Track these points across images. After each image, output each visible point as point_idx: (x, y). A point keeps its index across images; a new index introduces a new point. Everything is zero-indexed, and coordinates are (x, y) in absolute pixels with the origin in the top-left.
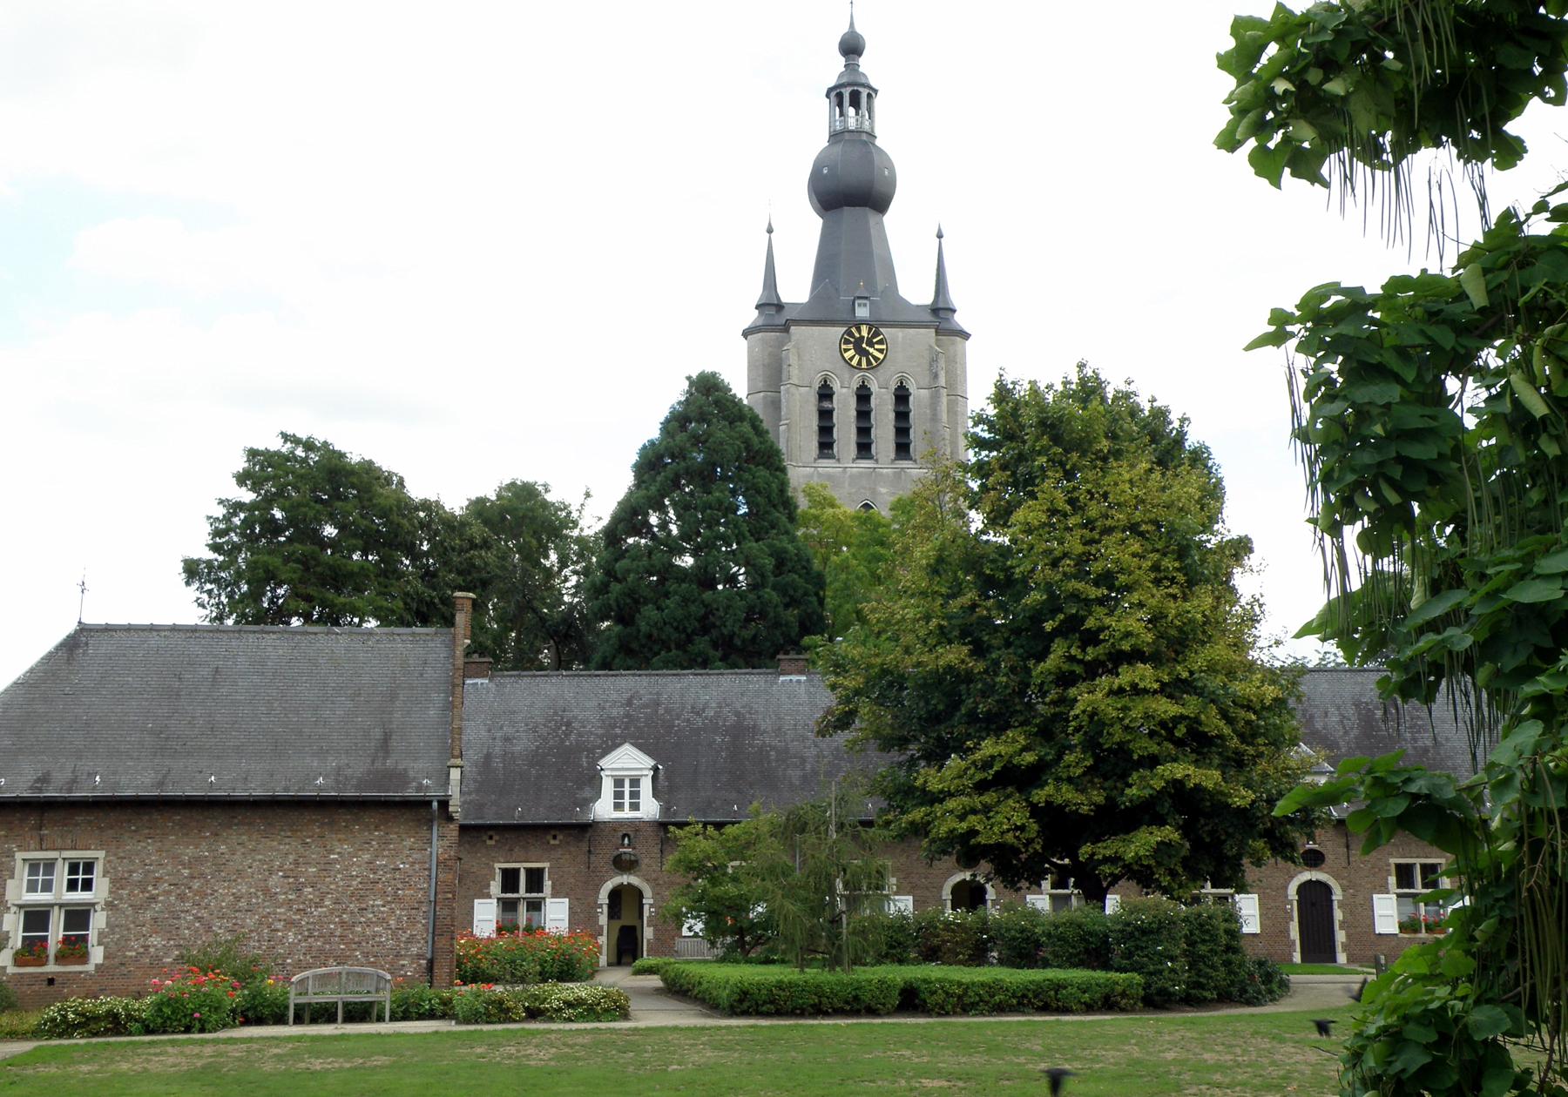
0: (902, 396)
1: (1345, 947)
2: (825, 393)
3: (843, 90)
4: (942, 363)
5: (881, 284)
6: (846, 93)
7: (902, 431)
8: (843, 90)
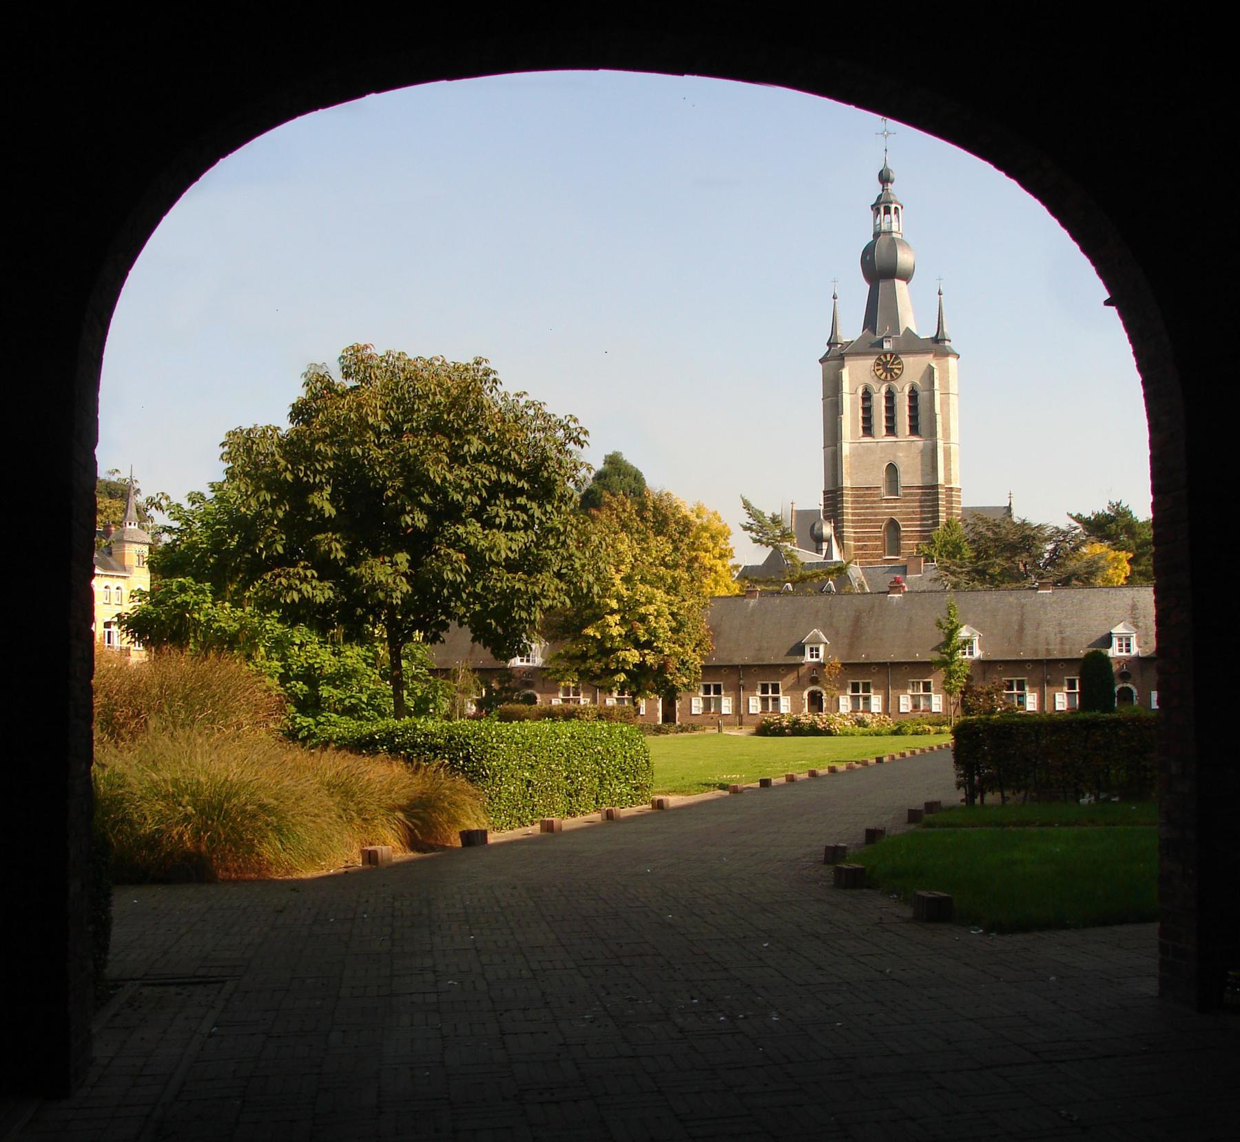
0: (913, 396)
2: (867, 396)
7: (914, 418)
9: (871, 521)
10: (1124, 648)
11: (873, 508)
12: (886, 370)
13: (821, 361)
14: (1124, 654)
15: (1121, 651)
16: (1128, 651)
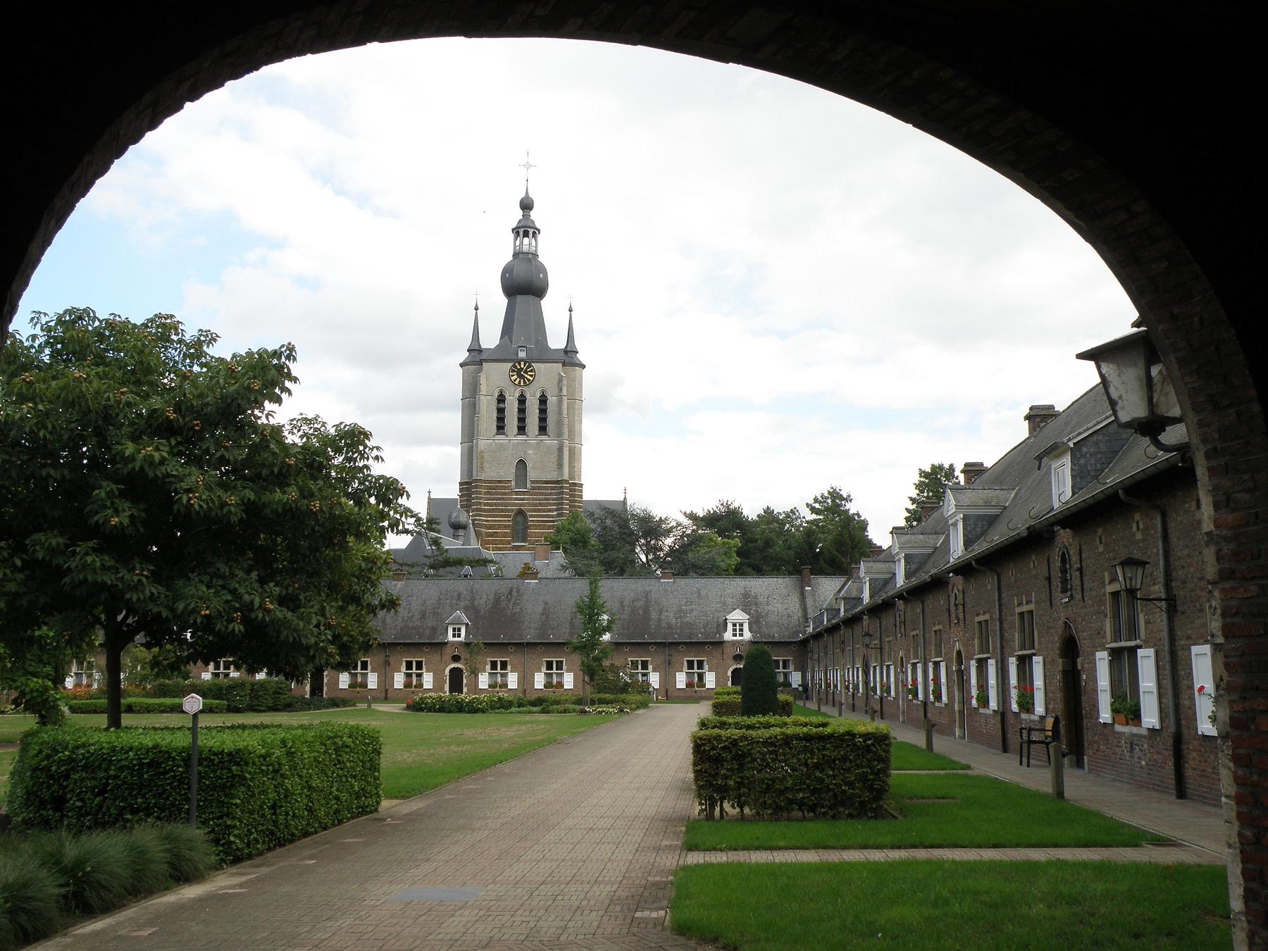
0: (543, 401)
2: (501, 399)
4: (565, 382)
7: (543, 419)
9: (502, 511)
10: (738, 632)
11: (503, 499)
13: (461, 365)
14: (738, 638)
15: (735, 635)
16: (741, 635)
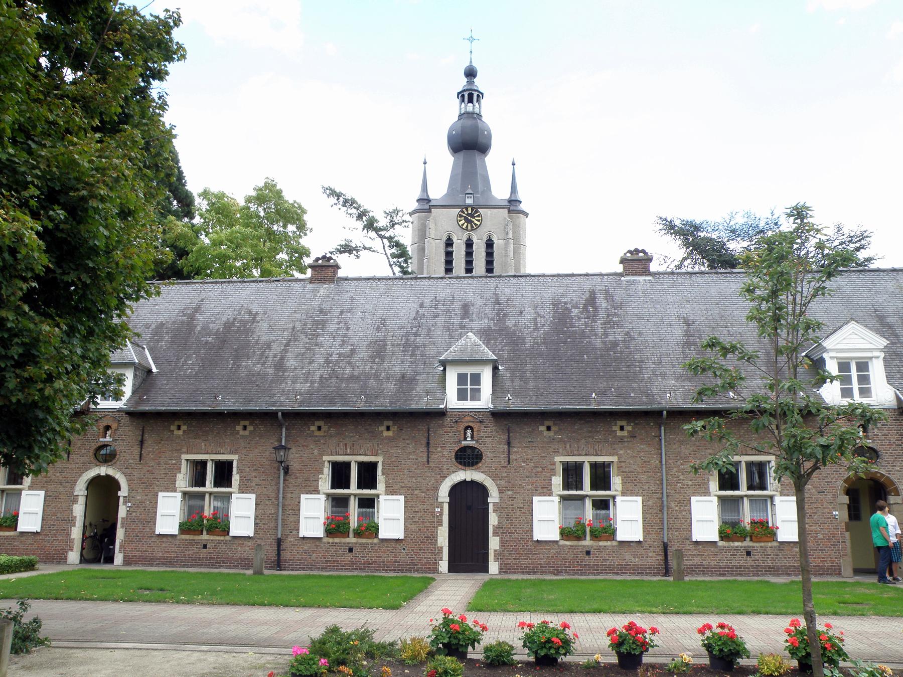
0: (490, 244)
1: (498, 556)
2: (449, 243)
3: (464, 93)
4: (511, 226)
5: (481, 187)
6: (466, 94)
7: (489, 263)
8: (464, 93)
12: (467, 220)
